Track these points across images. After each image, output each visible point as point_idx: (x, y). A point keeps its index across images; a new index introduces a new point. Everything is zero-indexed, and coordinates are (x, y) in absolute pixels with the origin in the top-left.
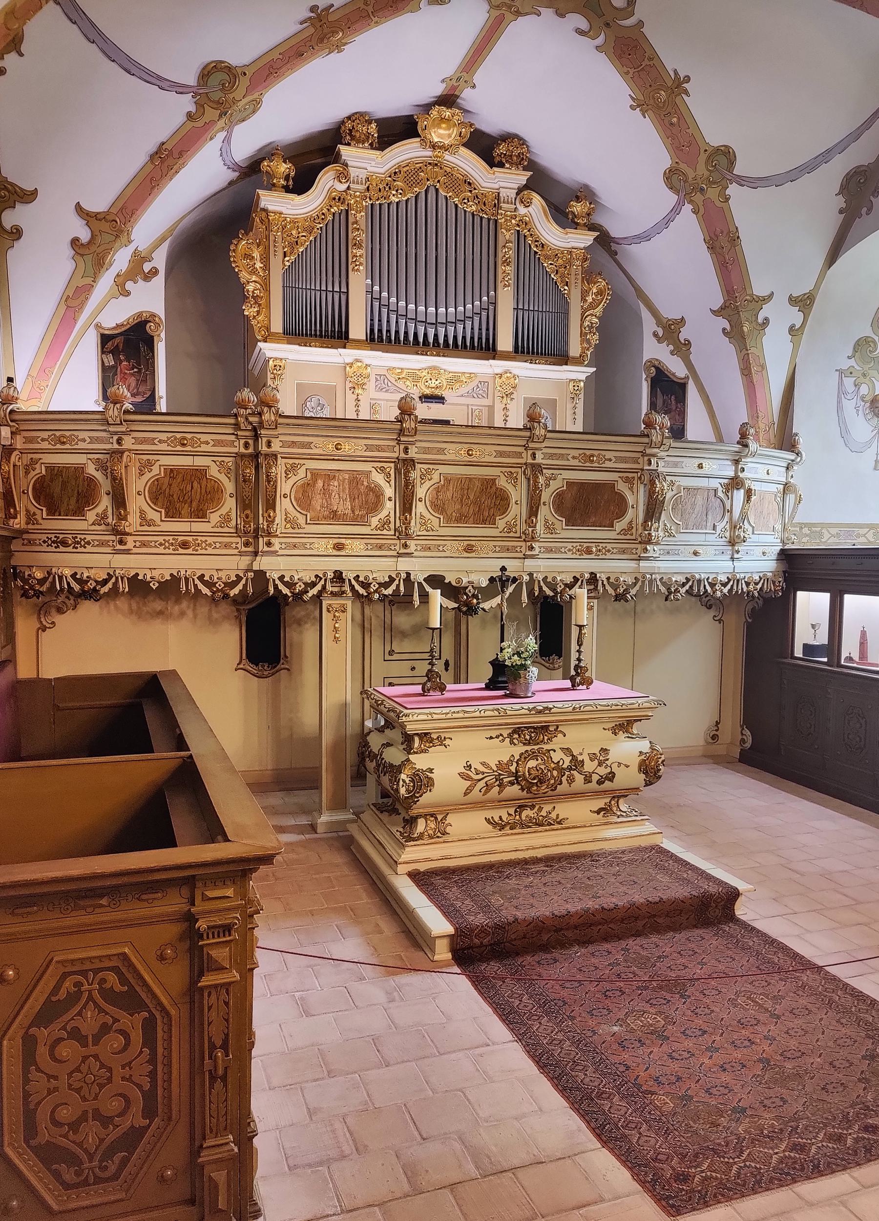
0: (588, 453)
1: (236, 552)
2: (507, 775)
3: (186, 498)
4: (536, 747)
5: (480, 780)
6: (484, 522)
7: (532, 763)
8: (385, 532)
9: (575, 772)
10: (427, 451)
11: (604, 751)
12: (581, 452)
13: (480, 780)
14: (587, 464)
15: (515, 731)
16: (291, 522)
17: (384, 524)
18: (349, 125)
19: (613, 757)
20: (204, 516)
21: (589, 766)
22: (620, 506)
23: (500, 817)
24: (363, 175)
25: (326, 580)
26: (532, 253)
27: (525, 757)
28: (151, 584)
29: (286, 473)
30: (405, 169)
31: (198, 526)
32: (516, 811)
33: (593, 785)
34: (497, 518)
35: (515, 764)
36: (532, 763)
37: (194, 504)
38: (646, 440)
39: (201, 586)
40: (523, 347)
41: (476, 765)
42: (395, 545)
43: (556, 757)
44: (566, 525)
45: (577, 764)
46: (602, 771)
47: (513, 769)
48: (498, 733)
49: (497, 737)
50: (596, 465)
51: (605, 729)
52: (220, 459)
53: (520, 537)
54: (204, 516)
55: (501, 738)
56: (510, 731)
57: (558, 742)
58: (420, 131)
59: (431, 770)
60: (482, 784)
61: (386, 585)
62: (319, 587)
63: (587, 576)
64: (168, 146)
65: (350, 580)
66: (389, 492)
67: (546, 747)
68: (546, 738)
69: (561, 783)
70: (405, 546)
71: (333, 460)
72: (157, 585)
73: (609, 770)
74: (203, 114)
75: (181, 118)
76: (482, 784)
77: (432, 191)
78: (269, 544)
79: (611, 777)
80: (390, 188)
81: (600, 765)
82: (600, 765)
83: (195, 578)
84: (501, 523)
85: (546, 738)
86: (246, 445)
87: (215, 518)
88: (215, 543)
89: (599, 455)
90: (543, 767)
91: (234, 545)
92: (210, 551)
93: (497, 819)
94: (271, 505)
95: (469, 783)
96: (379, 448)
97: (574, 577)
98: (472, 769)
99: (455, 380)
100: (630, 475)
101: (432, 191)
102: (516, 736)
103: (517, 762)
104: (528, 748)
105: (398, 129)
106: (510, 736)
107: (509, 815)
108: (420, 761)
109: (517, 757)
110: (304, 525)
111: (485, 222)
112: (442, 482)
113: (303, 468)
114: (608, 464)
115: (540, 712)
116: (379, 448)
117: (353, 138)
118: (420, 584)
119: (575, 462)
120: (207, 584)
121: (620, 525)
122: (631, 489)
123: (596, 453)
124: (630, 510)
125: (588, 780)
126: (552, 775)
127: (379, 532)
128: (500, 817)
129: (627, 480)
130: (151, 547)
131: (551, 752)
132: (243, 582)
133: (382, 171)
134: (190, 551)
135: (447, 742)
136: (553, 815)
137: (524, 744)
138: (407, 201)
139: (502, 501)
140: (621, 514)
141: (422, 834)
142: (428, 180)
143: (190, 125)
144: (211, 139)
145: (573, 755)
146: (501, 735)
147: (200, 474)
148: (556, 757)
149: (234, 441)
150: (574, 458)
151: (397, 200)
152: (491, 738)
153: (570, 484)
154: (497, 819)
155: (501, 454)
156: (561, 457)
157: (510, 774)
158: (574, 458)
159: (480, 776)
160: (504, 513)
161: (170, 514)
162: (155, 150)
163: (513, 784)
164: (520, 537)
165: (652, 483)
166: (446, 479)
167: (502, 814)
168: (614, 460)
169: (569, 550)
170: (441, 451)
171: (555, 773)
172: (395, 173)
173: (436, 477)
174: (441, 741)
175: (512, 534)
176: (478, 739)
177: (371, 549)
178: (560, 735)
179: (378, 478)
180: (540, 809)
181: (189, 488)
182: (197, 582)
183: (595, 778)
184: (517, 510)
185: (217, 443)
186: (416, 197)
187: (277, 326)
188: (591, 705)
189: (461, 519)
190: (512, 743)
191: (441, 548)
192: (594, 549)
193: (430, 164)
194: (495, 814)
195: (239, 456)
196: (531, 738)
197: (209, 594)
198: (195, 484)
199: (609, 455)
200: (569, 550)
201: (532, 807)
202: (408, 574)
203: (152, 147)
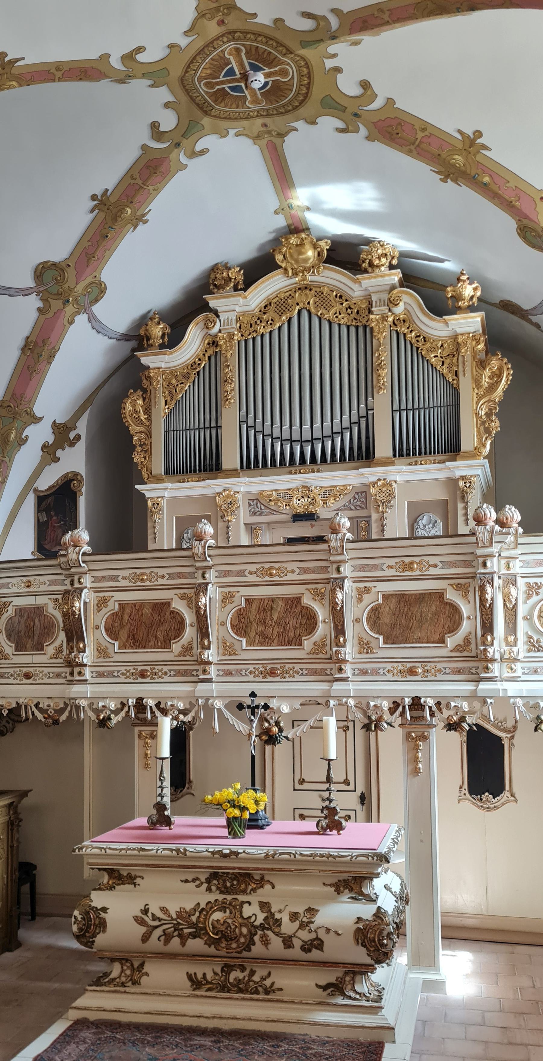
0: (407, 560)
1: (63, 681)
2: (187, 926)
3: (30, 634)
4: (229, 897)
5: (156, 927)
6: (289, 643)
7: (218, 916)
8: (188, 658)
9: (269, 933)
10: (226, 574)
11: (311, 911)
12: (398, 560)
13: (156, 927)
14: (407, 573)
15: (214, 876)
16: (102, 652)
17: (187, 649)
18: (212, 276)
19: (320, 919)
20: (42, 649)
21: (288, 927)
22: (454, 617)
23: (204, 974)
24: (233, 316)
25: (129, 707)
26: (415, 349)
27: (211, 907)
28: (3, 711)
29: (98, 607)
30: (275, 301)
31: (39, 659)
32: (222, 970)
33: (296, 952)
34: (303, 638)
35: (197, 914)
36: (218, 916)
37: (36, 638)
38: (473, 539)
39: (37, 713)
40: (414, 448)
41: (154, 909)
42: (197, 671)
43: (247, 911)
44: (385, 643)
45: (271, 922)
46: (305, 935)
47: (194, 918)
48: (194, 876)
49: (194, 880)
50: (418, 573)
51: (324, 884)
52: (55, 597)
53: (330, 659)
54: (42, 649)
55: (198, 882)
56: (207, 875)
57: (265, 893)
58: (279, 263)
59: (105, 910)
60: (158, 932)
61: (185, 712)
62: (123, 714)
63: (407, 701)
64: (33, 338)
65: (151, 707)
66: (189, 617)
67: (241, 898)
68: (250, 888)
69: (254, 944)
70: (205, 671)
71: (139, 590)
72: (7, 712)
73: (313, 936)
74: (50, 306)
75: (34, 315)
76: (158, 932)
77: (305, 315)
78: (80, 673)
79: (317, 944)
80: (261, 322)
81: (302, 926)
82: (302, 926)
83: (32, 706)
84: (308, 644)
85: (250, 888)
86: (72, 583)
87: (50, 650)
88: (49, 673)
89: (420, 563)
90: (230, 921)
91: (63, 675)
92: (46, 680)
93: (200, 976)
94: (81, 638)
95: (144, 929)
96: (180, 576)
97: (394, 702)
98: (150, 914)
99: (329, 493)
100: (462, 581)
101: (305, 315)
102: (215, 882)
103: (201, 912)
104: (221, 897)
105: (259, 267)
106: (208, 881)
107: (215, 974)
108: (98, 899)
109: (203, 905)
110: (113, 655)
111: (361, 330)
112: (244, 605)
113: (113, 599)
114: (433, 571)
115: (225, 856)
116: (180, 576)
117: (215, 285)
118: (219, 710)
119: (392, 572)
120: (41, 711)
121: (451, 642)
122: (465, 596)
123: (417, 559)
124: (465, 623)
125: (288, 942)
126: (241, 933)
127: (182, 658)
128: (204, 974)
129: (458, 587)
130: (5, 678)
131: (246, 906)
132: (69, 709)
133: (253, 306)
134: (30, 681)
135: (138, 881)
136: (268, 983)
137: (222, 892)
138: (280, 328)
139: (310, 621)
140: (455, 626)
141: (114, 980)
142: (298, 304)
143: (43, 317)
144: (71, 323)
145: (270, 911)
146: (197, 879)
147: (39, 611)
148: (247, 911)
149: (64, 580)
150: (390, 567)
151: (268, 330)
152: (186, 881)
153: (386, 597)
154: (200, 976)
155: (304, 571)
156: (375, 567)
157: (192, 925)
158: (390, 567)
159: (156, 923)
160: (311, 632)
161: (19, 648)
162: (23, 343)
163: (195, 937)
164: (330, 659)
165: (482, 589)
166: (247, 600)
167: (207, 970)
168: (440, 565)
169: (389, 671)
170: (241, 573)
171: (245, 930)
172: (265, 307)
173: (236, 600)
174: (131, 879)
175: (321, 656)
176: (172, 881)
177: (174, 676)
178: (268, 887)
179: (179, 606)
180: (253, 973)
181: (32, 624)
182: (34, 709)
183: (297, 943)
184: (323, 629)
185: (52, 583)
186: (289, 321)
187: (159, 466)
188: (289, 854)
189: (265, 640)
190: (209, 890)
191: (243, 673)
192: (420, 670)
193: (300, 289)
194: (199, 970)
195: (67, 592)
196: (232, 885)
197: (43, 720)
198: (36, 620)
199: (432, 560)
200: (389, 671)
201: (243, 969)
202: (207, 699)
203: (20, 342)
